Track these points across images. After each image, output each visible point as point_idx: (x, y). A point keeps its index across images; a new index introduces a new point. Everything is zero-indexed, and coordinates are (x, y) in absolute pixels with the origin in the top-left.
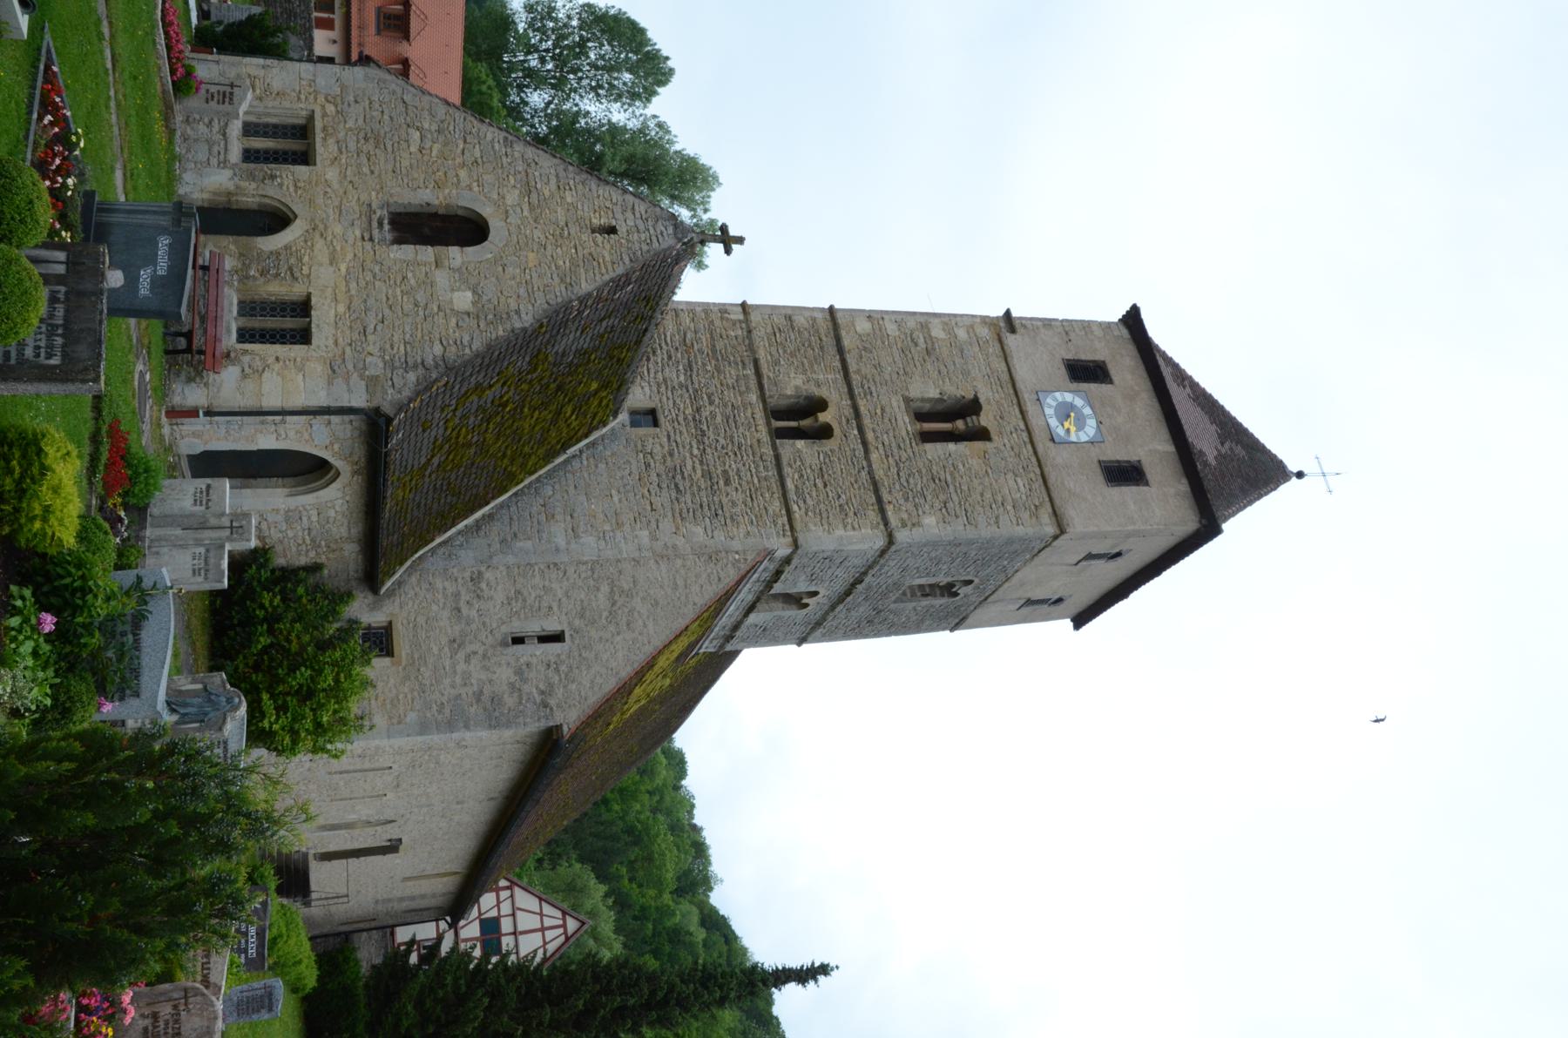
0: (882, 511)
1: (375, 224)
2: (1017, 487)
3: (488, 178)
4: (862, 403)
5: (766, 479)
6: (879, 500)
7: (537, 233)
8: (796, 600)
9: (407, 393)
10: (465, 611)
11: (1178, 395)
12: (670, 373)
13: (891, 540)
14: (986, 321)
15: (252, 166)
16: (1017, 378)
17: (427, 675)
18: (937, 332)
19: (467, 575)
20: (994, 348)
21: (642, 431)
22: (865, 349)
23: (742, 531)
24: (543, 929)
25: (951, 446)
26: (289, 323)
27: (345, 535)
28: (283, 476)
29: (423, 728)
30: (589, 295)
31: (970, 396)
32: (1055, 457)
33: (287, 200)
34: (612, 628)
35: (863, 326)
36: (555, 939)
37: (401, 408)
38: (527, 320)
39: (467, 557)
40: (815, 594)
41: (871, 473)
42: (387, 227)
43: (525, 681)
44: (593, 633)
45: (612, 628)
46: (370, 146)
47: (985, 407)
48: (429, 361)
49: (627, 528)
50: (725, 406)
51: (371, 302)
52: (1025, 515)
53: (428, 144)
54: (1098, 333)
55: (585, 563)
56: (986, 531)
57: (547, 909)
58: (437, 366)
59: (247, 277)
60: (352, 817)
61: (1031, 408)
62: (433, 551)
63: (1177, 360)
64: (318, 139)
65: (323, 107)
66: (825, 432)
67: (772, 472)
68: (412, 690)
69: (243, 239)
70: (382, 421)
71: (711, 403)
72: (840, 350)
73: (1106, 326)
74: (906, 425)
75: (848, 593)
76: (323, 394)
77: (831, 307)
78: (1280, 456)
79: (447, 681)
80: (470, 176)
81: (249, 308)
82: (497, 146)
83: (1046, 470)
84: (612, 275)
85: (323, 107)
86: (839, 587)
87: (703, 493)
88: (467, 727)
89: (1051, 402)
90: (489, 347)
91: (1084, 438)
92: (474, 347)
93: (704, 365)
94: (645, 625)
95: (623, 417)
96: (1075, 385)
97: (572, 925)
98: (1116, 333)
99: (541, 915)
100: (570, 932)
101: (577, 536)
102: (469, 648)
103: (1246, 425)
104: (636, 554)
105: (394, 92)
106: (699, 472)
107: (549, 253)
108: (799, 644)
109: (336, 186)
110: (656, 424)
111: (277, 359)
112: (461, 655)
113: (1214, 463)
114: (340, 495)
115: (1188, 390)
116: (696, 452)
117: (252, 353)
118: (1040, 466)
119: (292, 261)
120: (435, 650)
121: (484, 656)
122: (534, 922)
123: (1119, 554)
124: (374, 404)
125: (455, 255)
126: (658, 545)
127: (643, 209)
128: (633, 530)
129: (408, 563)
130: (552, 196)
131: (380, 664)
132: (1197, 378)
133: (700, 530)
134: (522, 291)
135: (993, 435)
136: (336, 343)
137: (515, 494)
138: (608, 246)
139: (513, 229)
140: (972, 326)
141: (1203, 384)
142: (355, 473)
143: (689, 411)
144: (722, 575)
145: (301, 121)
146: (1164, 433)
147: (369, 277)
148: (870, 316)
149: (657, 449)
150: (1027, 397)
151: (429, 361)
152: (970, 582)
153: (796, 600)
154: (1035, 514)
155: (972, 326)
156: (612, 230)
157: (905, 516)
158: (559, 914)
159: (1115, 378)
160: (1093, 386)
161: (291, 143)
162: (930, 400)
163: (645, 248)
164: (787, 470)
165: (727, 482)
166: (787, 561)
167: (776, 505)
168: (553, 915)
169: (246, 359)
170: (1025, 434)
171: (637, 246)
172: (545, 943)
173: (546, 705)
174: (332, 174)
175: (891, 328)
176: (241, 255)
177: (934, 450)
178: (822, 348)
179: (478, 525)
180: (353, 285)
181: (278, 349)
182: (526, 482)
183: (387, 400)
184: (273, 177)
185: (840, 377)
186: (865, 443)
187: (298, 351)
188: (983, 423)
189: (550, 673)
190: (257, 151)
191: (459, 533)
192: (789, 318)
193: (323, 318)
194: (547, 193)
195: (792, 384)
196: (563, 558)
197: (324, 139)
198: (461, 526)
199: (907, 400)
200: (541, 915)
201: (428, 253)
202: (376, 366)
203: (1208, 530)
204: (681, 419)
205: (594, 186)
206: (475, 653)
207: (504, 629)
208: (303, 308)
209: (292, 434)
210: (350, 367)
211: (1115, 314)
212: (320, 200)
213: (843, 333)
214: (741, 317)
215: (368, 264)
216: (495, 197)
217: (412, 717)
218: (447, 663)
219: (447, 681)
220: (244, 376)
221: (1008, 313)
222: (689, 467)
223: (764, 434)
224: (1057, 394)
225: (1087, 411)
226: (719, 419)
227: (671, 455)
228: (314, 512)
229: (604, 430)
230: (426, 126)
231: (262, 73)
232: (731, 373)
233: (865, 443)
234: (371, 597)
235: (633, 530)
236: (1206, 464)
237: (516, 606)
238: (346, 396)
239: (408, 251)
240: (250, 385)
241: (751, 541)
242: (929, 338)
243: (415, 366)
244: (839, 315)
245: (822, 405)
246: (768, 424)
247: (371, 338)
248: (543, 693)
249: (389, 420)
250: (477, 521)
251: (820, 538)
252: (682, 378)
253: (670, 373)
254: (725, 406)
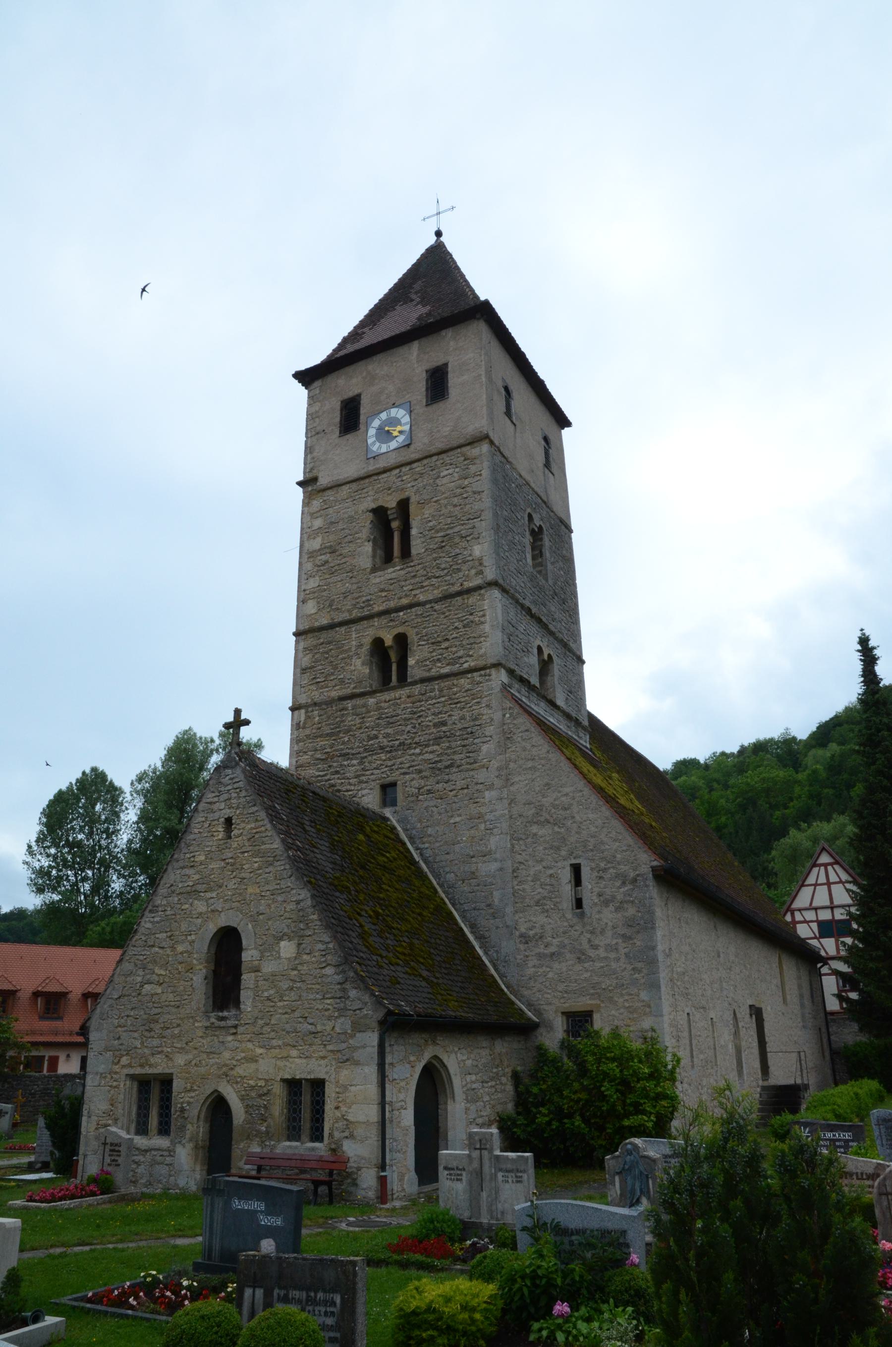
0: (469, 591)
1: (223, 1023)
2: (448, 477)
3: (184, 926)
4: (377, 608)
5: (441, 691)
6: (459, 594)
7: (231, 885)
8: (545, 665)
9: (367, 998)
10: (552, 949)
11: (370, 338)
12: (350, 772)
13: (494, 584)
14: (306, 503)
15: (173, 1128)
16: (356, 475)
17: (608, 982)
18: (316, 544)
19: (522, 947)
20: (330, 495)
21: (400, 796)
22: (330, 605)
23: (485, 711)
24: (829, 884)
25: (414, 532)
26: (306, 1098)
27: (487, 1051)
28: (437, 1104)
29: (654, 986)
30: (283, 841)
31: (370, 516)
32: (422, 443)
33: (202, 1098)
34: (569, 823)
35: (311, 607)
36: (837, 873)
37: (379, 1002)
38: (305, 894)
39: (507, 946)
40: (540, 649)
41: (437, 601)
42: (225, 1014)
43: (614, 897)
44: (572, 840)
45: (569, 823)
46: (157, 1027)
47: (380, 503)
48: (339, 978)
49: (483, 810)
50: (378, 725)
51: (288, 1027)
52: (473, 469)
53: (155, 977)
54: (317, 407)
55: (513, 846)
56: (486, 502)
57: (811, 880)
58: (343, 972)
59: (267, 1132)
60: (731, 1048)
61: (382, 464)
62: (502, 976)
63: (339, 340)
64: (151, 1071)
65: (123, 1066)
66: (402, 640)
67: (436, 685)
68: (622, 995)
69: (235, 1135)
70: (391, 1019)
71: (376, 737)
72: (331, 626)
73: (311, 398)
74: (393, 572)
75: (539, 621)
76: (366, 1069)
77: (294, 634)
78: (423, 251)
79: (614, 965)
80: (183, 942)
81: (293, 1133)
82: (157, 919)
83: (434, 451)
84: (266, 821)
85: (123, 1066)
86: (534, 628)
87: (453, 744)
88: (653, 948)
89: (377, 447)
90: (328, 927)
91: (407, 419)
92: (327, 939)
93: (344, 743)
94: (567, 795)
95: (388, 812)
96: (362, 427)
97: (825, 859)
98: (317, 391)
99: (816, 885)
100: (832, 860)
101: (490, 853)
102: (586, 946)
103: (396, 281)
104: (506, 802)
105: (111, 1006)
106: (435, 748)
107: (247, 875)
108: (583, 662)
109: (190, 1056)
110: (394, 785)
111: (337, 1108)
112: (592, 953)
113: (428, 308)
114: (453, 1056)
115: (366, 330)
116: (417, 751)
117: (331, 1129)
118: (431, 456)
119: (253, 1094)
120: (587, 975)
121: (592, 933)
122: (822, 892)
123: (506, 389)
124: (375, 1025)
125: (249, 955)
126: (498, 783)
127: (210, 795)
128: (484, 804)
129: (512, 997)
130: (198, 872)
131: (599, 1023)
132: (356, 322)
133: (485, 748)
134: (280, 898)
135: (403, 496)
136: (323, 1058)
137: (453, 905)
138: (243, 825)
139: (227, 906)
140: (312, 514)
141: (361, 317)
142: (434, 1043)
143: (383, 756)
144: (523, 728)
145: (135, 1085)
146: (402, 351)
147: (267, 1029)
148: (302, 601)
149: (415, 783)
150: (372, 467)
151: (339, 978)
152: (530, 516)
153: (545, 665)
154: (472, 460)
155: (312, 514)
156: (229, 822)
157: (473, 572)
158: (815, 870)
159: (356, 392)
160: (363, 411)
161: (154, 1095)
162: (374, 550)
163: (243, 793)
164: (433, 672)
165: (444, 724)
166: (511, 672)
167: (463, 682)
168: (816, 875)
169: (337, 1135)
170: (405, 469)
171: (242, 800)
172: (841, 882)
173: (634, 881)
174: (180, 1060)
175: (313, 583)
176: (248, 1138)
177: (417, 546)
178: (330, 643)
179: (479, 938)
180: (275, 1043)
181: (329, 1107)
182: (443, 896)
183: (372, 1014)
184: (183, 1110)
185: (354, 628)
186: (411, 606)
187: (330, 1091)
188: (394, 504)
189: (607, 876)
190: (160, 1123)
191: (486, 953)
192: (304, 671)
193: (301, 1067)
194: (197, 877)
195: (360, 667)
196: (509, 864)
197: (151, 1066)
198: (480, 952)
199: (374, 570)
200: (816, 885)
201: (247, 979)
202: (343, 1024)
203: (486, 312)
204: (389, 763)
205: (192, 837)
206: (590, 941)
207: (569, 916)
208: (293, 1085)
209: (402, 1096)
210: (344, 1045)
211: (301, 393)
212: (202, 1070)
213: (317, 624)
214: (303, 711)
215: (257, 1029)
216: (199, 921)
217: (644, 995)
218: (598, 964)
219: (614, 965)
220: (351, 1136)
221: (300, 484)
222: (431, 756)
223: (404, 692)
224: (370, 441)
225: (384, 416)
226: (389, 731)
227: (420, 771)
228: (468, 1078)
229: (399, 829)
230: (139, 979)
231: (94, 1118)
232: (350, 720)
233: (411, 606)
234: (542, 1030)
235: (484, 804)
236: (429, 314)
237: (549, 905)
238: (369, 1049)
239: (246, 997)
240: (359, 1132)
241: (494, 704)
242: (321, 551)
243: (344, 990)
244: (302, 628)
245: (378, 643)
246: (394, 688)
247: (319, 1028)
248: (624, 883)
249: (390, 1013)
250: (476, 938)
251: (492, 645)
252: (355, 762)
253: (350, 772)
254: (378, 725)
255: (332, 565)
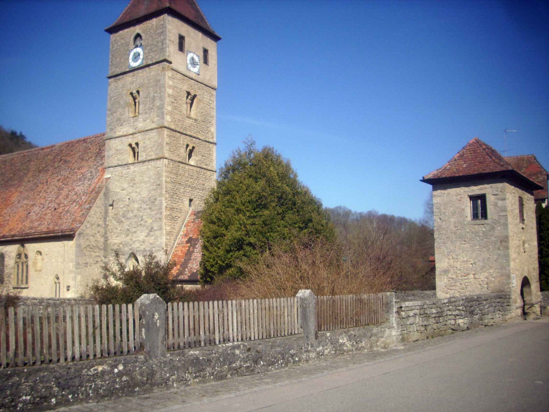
41: (203, 141)
52: (212, 98)
72: (175, 131)
150: (187, 73)
164: (202, 166)
170: (196, 83)
186: (197, 138)
233: (197, 138)
255: (175, 105)
